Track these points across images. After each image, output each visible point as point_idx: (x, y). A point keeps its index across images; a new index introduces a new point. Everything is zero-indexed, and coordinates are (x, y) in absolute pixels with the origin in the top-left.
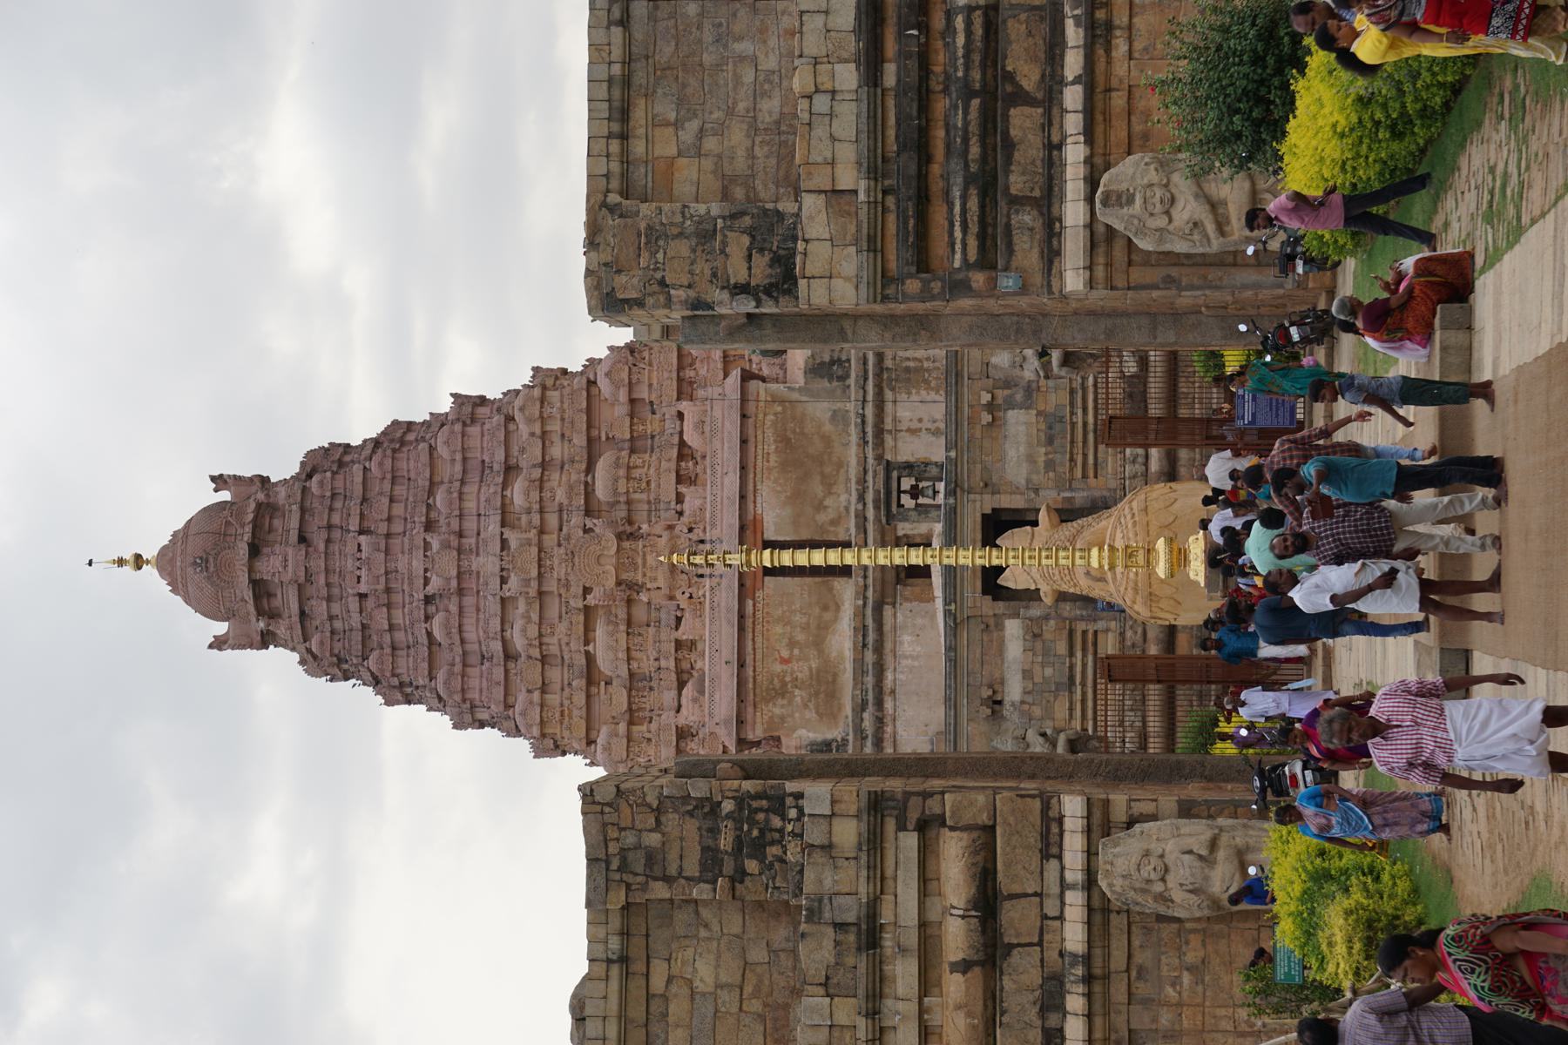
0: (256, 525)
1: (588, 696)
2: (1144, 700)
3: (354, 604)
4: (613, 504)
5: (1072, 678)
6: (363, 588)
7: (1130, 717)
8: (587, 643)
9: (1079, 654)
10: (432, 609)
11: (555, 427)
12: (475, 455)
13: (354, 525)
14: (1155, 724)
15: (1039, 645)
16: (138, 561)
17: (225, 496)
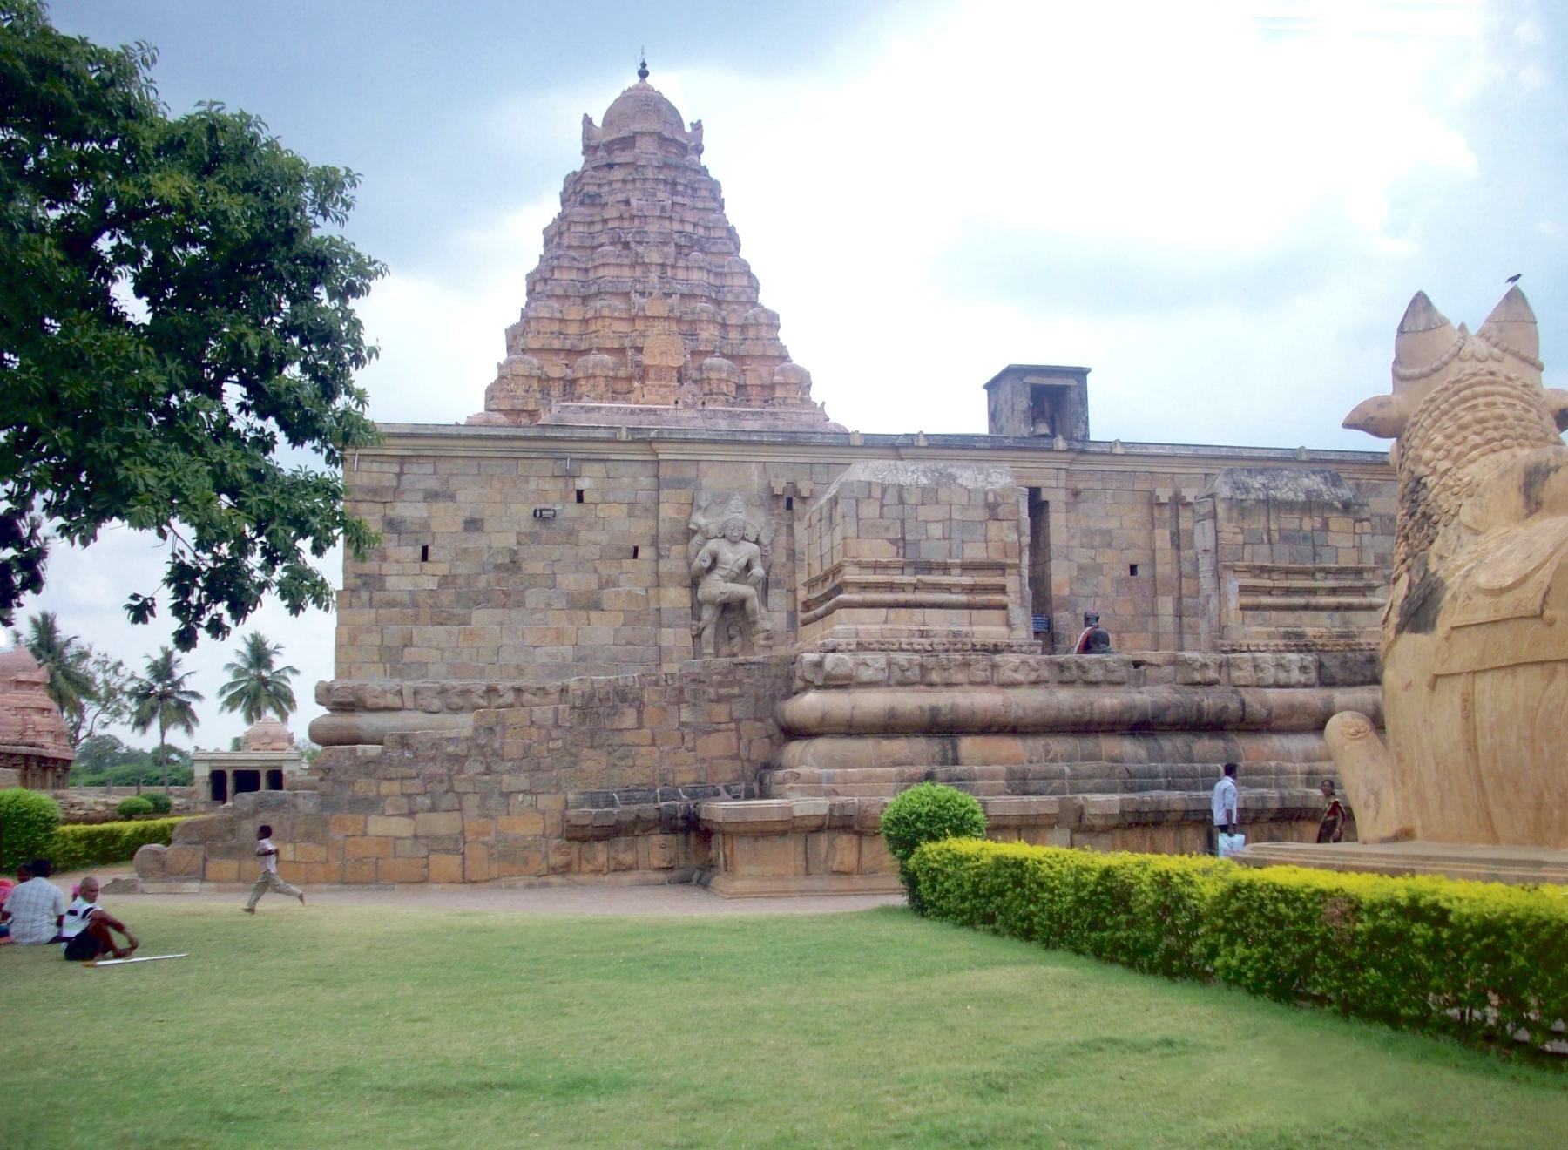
0: (673, 141)
1: (558, 351)
2: (904, 684)
3: (620, 197)
4: (700, 369)
5: (928, 567)
6: (634, 202)
7: (879, 660)
8: (598, 349)
9: (966, 580)
10: (619, 247)
11: (752, 333)
12: (728, 281)
13: (679, 199)
14: (873, 702)
15: (980, 514)
16: (643, 74)
17: (688, 129)
